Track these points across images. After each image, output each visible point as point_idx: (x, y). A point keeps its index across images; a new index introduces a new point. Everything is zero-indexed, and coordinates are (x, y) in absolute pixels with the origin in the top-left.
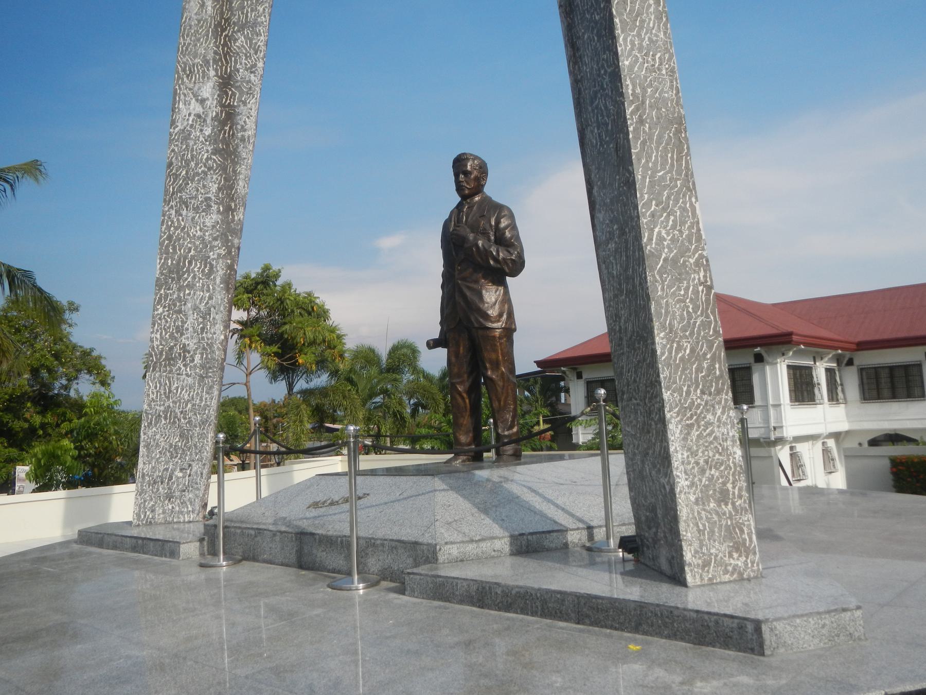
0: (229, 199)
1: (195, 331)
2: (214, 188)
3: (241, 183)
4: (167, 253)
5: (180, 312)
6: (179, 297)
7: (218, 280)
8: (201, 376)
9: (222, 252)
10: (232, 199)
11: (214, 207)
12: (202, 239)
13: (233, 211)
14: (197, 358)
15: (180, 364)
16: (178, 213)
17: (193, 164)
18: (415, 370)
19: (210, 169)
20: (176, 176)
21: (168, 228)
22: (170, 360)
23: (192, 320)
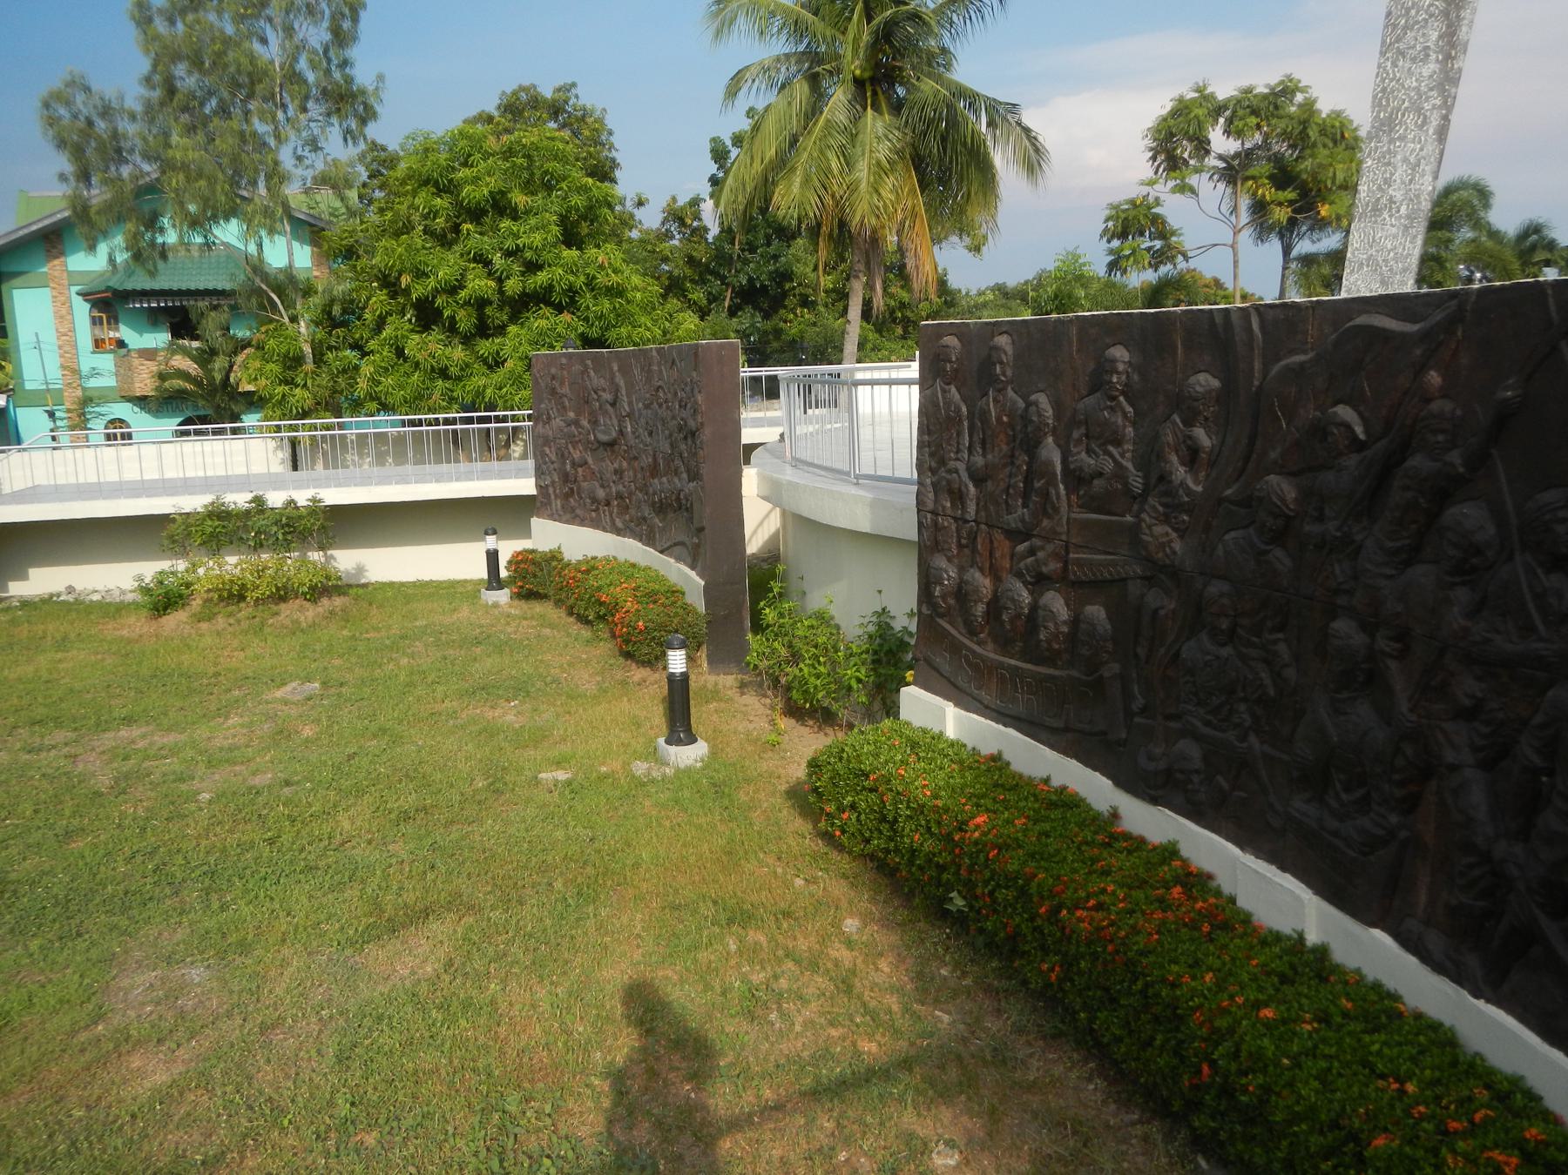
0: (1451, 45)
1: (1403, 182)
2: (1434, 35)
3: (1464, 29)
4: (1380, 105)
5: (1389, 164)
6: (1389, 151)
7: (1431, 131)
8: (1406, 228)
9: (1438, 102)
10: (1453, 45)
11: (1433, 56)
12: (1417, 89)
13: (1453, 58)
14: (1403, 210)
15: (1386, 215)
16: (1394, 65)
17: (1413, 12)
18: (1478, 224)
19: (1431, 16)
20: (1395, 26)
21: (1383, 80)
22: (1376, 211)
23: (1401, 173)
